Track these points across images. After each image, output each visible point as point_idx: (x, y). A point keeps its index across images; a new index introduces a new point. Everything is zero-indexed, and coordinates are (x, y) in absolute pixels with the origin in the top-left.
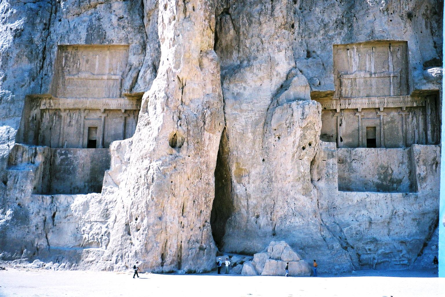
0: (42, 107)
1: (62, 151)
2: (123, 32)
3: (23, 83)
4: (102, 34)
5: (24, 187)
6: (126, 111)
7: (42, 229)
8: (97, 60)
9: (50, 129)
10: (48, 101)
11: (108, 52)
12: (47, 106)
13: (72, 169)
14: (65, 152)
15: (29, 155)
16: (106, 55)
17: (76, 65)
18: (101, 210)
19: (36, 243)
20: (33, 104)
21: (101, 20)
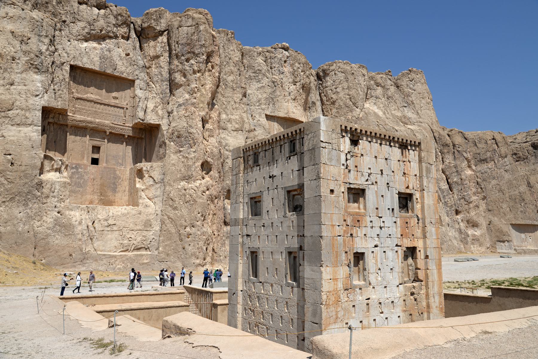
0: (51, 120)
2: (130, 68)
3: (38, 93)
4: (114, 65)
5: (63, 196)
10: (57, 115)
13: (83, 183)
15: (57, 165)
19: (84, 249)
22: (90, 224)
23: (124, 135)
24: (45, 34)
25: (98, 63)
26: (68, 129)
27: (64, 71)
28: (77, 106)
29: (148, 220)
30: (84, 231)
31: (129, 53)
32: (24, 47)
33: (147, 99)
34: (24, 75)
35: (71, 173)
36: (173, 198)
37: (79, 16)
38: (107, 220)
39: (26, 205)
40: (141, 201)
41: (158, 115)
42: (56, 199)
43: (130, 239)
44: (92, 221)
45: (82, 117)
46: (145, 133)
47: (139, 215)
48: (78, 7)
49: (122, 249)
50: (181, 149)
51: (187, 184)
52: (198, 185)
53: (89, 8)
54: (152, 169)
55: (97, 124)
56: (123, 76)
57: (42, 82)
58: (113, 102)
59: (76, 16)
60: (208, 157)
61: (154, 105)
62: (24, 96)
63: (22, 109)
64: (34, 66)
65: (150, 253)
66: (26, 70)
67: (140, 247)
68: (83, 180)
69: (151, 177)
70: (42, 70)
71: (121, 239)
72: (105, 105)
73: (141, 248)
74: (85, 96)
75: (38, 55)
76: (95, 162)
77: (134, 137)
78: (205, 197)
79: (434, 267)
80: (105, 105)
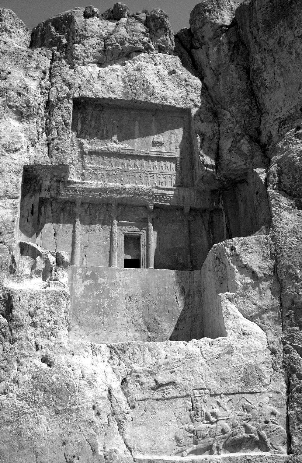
1: (87, 270)
2: (178, 91)
3: (17, 146)
4: (148, 88)
5: (52, 322)
6: (191, 210)
7: (110, 412)
8: (137, 128)
9: (55, 235)
10: (55, 184)
11: (153, 118)
12: (53, 193)
13: (108, 306)
14: (93, 274)
16: (151, 122)
17: (101, 132)
18: (242, 370)
19: (100, 448)
20: (28, 187)
21: (143, 71)
22: (116, 385)
23: (182, 209)
24: (35, 66)
25: (121, 88)
26: (76, 210)
28: (89, 165)
29: (251, 366)
30: (100, 402)
33: (217, 136)
35: (83, 288)
37: (86, 31)
40: (229, 324)
41: (239, 152)
43: (213, 419)
44: (121, 378)
46: (224, 200)
47: (228, 357)
54: (245, 250)
55: (128, 193)
56: (167, 104)
58: (154, 151)
61: (232, 139)
64: (15, 109)
68: (107, 300)
70: (27, 114)
71: (189, 420)
72: (140, 157)
73: (243, 440)
75: (21, 92)
77: (205, 211)
80: (140, 157)
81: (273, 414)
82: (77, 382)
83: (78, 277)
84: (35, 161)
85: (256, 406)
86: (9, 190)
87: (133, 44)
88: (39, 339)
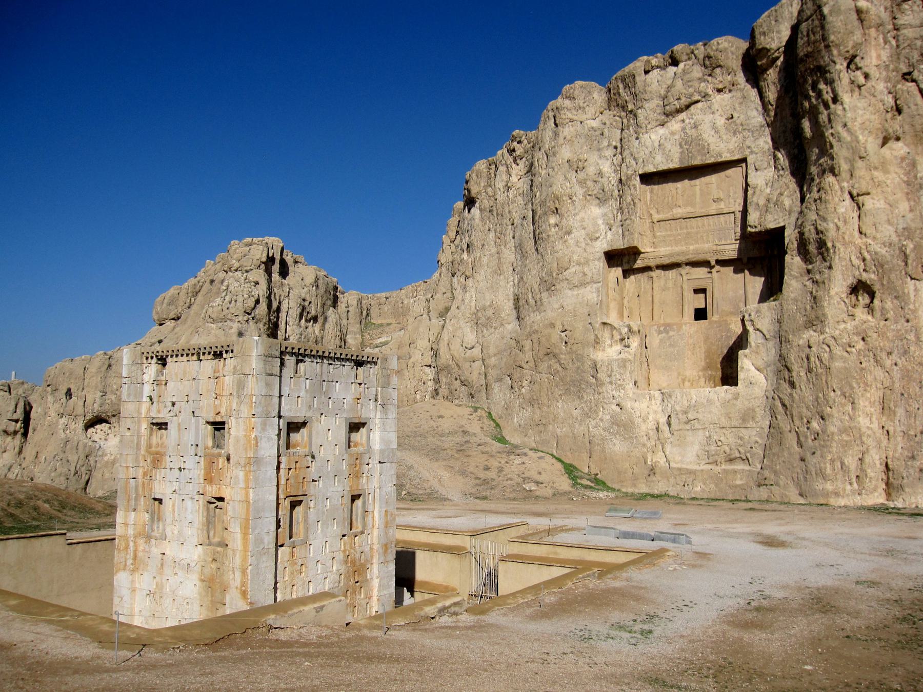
1: (660, 327)
2: (734, 139)
3: (597, 235)
4: (703, 148)
18: (743, 412)
22: (663, 420)
24: (606, 144)
25: (678, 155)
27: (632, 188)
29: (749, 409)
30: (650, 432)
31: (732, 115)
32: (581, 175)
33: (769, 185)
34: (582, 215)
36: (789, 365)
38: (686, 413)
39: (580, 398)
40: (741, 376)
42: (614, 386)
43: (719, 443)
45: (668, 248)
47: (735, 402)
48: (645, 81)
49: (707, 461)
50: (810, 267)
51: (815, 334)
52: (837, 332)
53: (663, 72)
57: (605, 215)
59: (642, 97)
60: (864, 270)
61: (779, 191)
62: (583, 245)
63: (579, 264)
65: (747, 468)
66: (584, 207)
67: (733, 456)
69: (758, 330)
73: (736, 458)
74: (669, 216)
76: (701, 314)
78: (853, 357)
79: (238, 530)
81: (757, 442)
82: (636, 420)
83: (654, 332)
84: (611, 246)
85: (747, 437)
86: (594, 276)
87: (690, 98)
88: (614, 392)
